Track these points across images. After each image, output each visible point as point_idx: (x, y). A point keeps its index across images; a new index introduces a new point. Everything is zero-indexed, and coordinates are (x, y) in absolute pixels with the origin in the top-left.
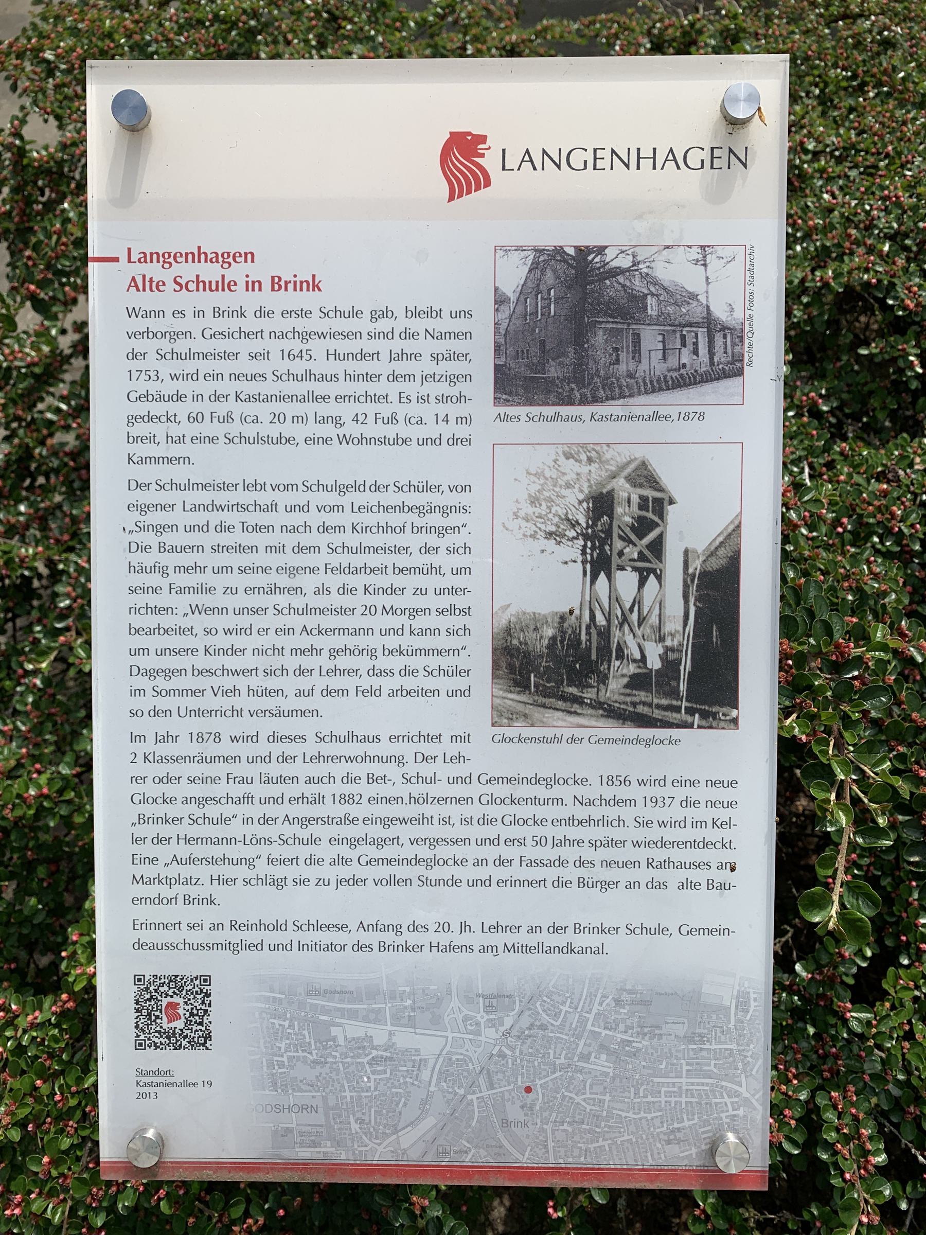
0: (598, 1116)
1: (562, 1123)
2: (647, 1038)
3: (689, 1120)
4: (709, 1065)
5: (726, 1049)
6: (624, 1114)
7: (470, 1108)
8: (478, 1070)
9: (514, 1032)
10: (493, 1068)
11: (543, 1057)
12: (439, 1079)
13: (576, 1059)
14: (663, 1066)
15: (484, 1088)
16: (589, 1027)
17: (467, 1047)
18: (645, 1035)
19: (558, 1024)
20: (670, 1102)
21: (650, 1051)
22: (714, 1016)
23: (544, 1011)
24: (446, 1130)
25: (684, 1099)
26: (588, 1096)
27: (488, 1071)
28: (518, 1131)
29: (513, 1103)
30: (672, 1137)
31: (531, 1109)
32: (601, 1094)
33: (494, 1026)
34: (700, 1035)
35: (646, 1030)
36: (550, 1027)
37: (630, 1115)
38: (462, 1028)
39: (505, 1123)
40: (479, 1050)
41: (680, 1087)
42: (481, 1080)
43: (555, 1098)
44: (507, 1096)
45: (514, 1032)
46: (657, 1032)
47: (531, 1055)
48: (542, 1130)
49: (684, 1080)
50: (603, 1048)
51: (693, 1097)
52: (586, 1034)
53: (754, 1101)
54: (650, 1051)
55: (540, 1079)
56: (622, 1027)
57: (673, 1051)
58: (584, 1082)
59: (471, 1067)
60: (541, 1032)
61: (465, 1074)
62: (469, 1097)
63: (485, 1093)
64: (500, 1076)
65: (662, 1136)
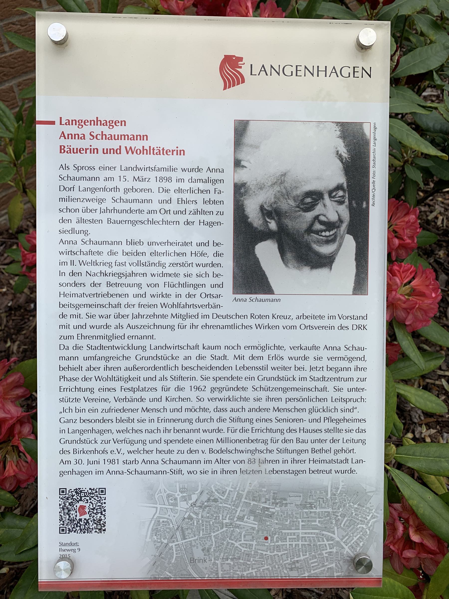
0: (248, 555)
1: (227, 559)
2: (278, 506)
3: (303, 555)
4: (315, 521)
5: (325, 512)
6: (264, 553)
7: (171, 551)
8: (176, 527)
9: (198, 504)
10: (185, 526)
11: (216, 519)
12: (152, 534)
13: (235, 519)
14: (288, 523)
15: (179, 538)
16: (243, 500)
17: (169, 513)
18: (277, 504)
19: (224, 498)
20: (292, 545)
21: (280, 514)
22: (318, 492)
23: (216, 490)
24: (157, 564)
25: (300, 543)
26: (243, 542)
27: (182, 528)
28: (200, 565)
29: (197, 548)
30: (293, 566)
31: (208, 551)
32: (251, 540)
33: (185, 500)
34: (310, 503)
35: (278, 501)
36: (219, 500)
37: (268, 553)
38: (166, 503)
39: (193, 560)
40: (177, 515)
41: (298, 536)
42: (178, 533)
43: (223, 544)
44: (193, 543)
45: (198, 504)
46: (284, 502)
47: (208, 517)
48: (215, 564)
49: (300, 531)
50: (252, 512)
51: (306, 541)
52: (241, 504)
53: (342, 543)
54: (280, 514)
55: (214, 532)
56: (263, 500)
57: (294, 513)
58: (240, 533)
59: (171, 526)
60: (214, 503)
61: (168, 530)
62: (171, 545)
63: (180, 542)
64: (190, 531)
65: (287, 566)
